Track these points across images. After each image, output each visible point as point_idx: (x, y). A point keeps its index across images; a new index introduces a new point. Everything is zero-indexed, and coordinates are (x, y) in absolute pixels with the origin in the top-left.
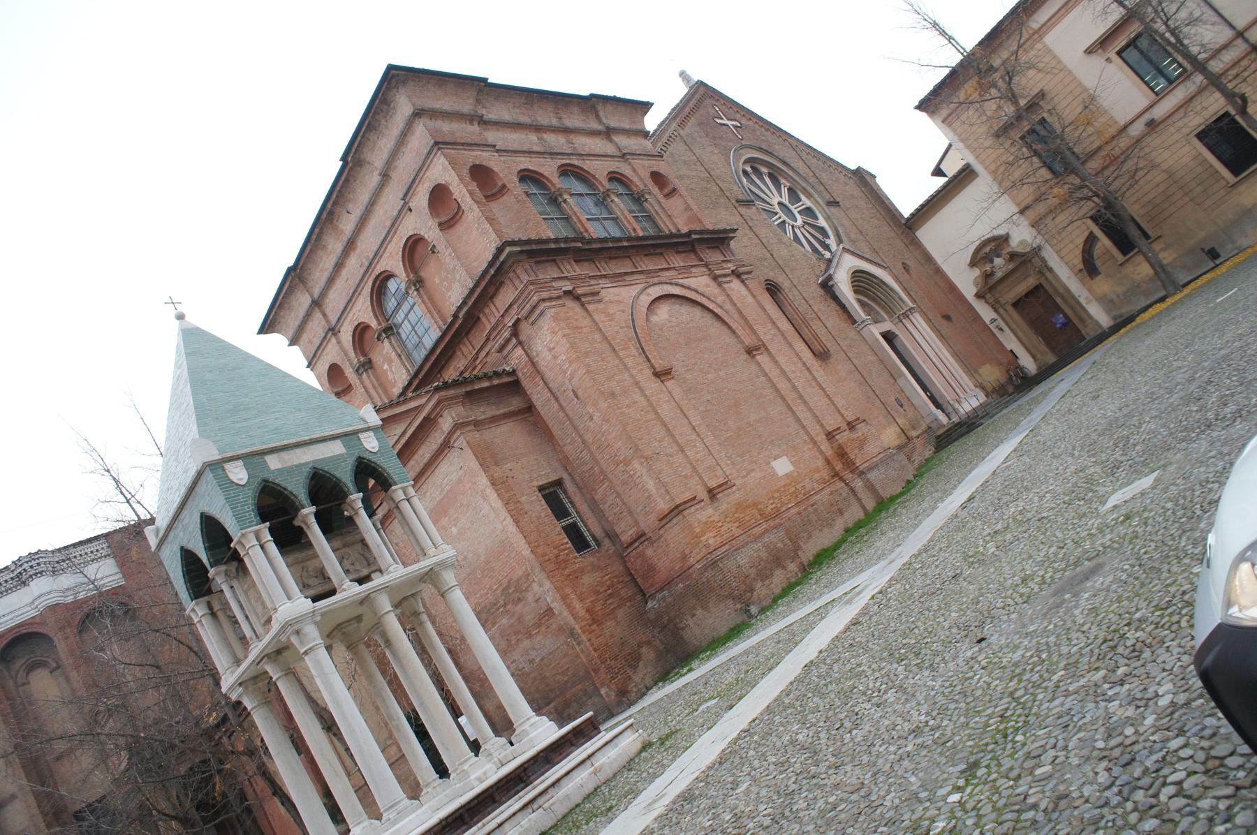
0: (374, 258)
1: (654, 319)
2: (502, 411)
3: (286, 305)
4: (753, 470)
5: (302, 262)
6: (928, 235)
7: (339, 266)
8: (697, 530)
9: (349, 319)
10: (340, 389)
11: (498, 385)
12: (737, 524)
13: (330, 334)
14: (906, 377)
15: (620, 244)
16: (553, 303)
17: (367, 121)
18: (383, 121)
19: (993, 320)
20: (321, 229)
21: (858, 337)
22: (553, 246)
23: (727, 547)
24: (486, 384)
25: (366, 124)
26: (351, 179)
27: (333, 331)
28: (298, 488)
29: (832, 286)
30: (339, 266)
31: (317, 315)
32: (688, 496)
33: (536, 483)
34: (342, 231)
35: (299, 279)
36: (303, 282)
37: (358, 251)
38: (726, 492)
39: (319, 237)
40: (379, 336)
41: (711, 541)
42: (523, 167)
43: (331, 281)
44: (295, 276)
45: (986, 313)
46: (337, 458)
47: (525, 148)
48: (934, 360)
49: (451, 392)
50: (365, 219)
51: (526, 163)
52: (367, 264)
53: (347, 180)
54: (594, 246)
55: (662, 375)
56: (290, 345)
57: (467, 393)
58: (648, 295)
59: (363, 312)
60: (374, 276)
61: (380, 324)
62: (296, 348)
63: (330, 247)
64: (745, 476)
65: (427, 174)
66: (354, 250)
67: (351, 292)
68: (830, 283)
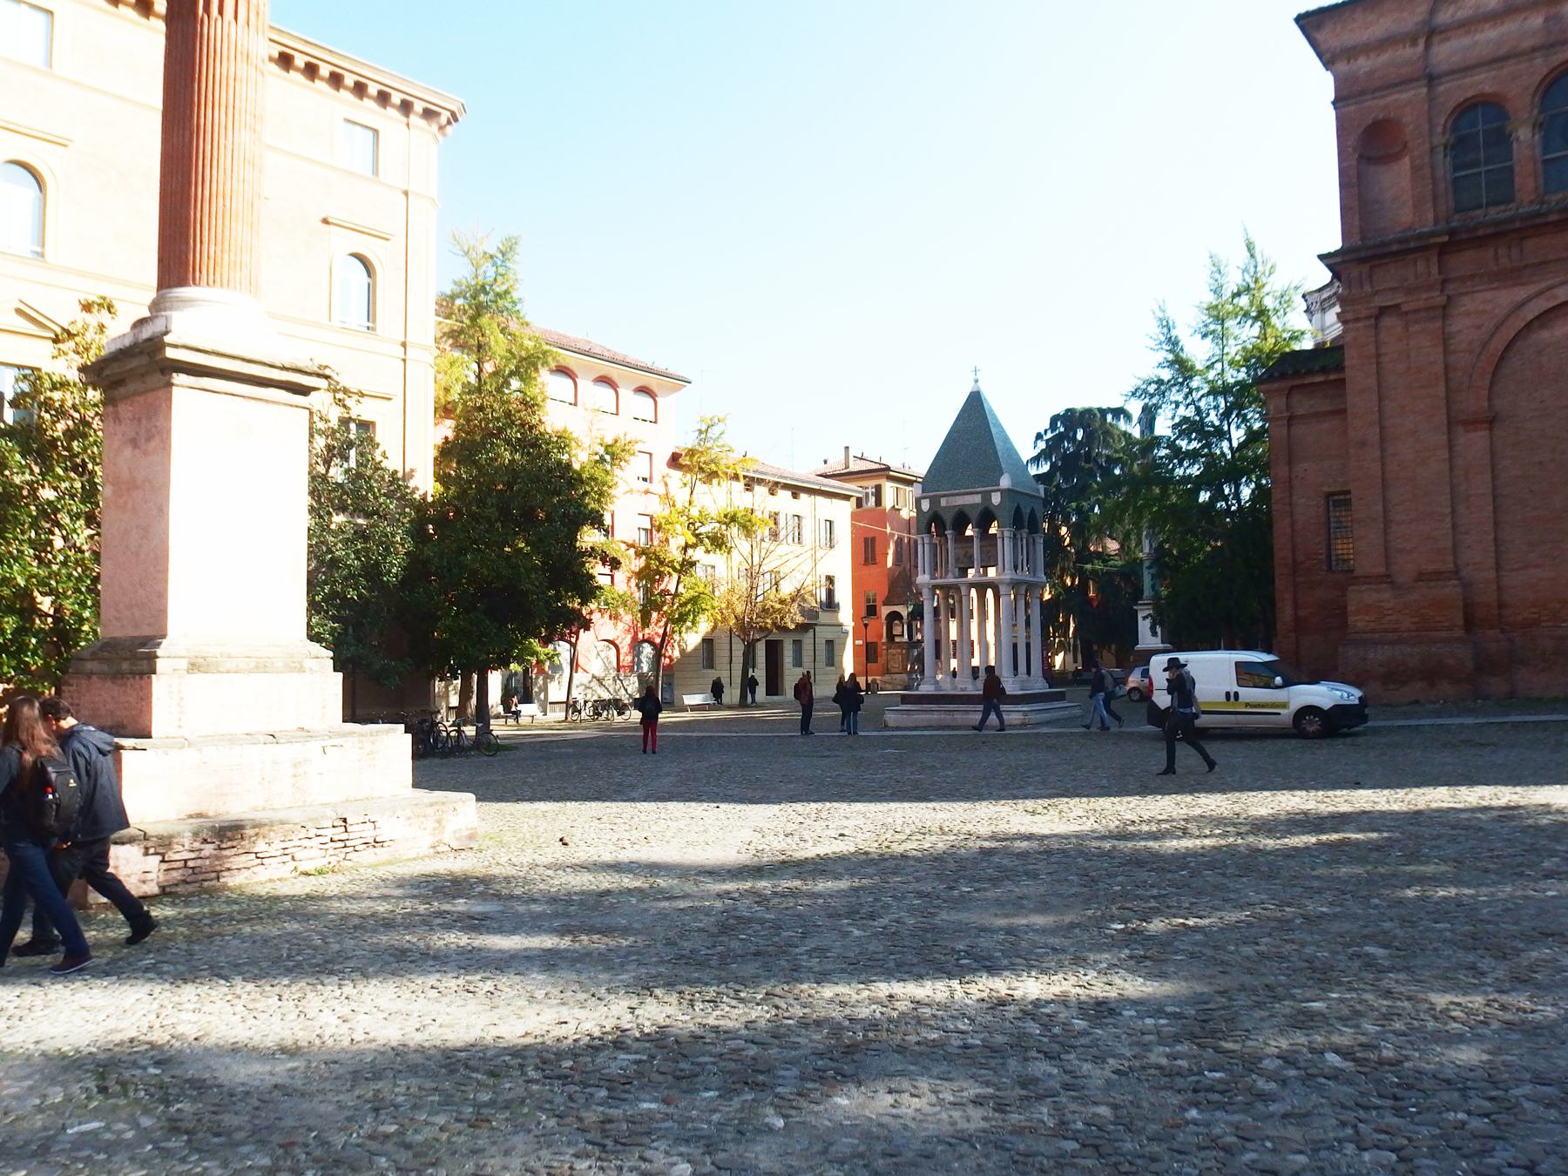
1: (1545, 335)
2: (1329, 408)
4: (1536, 566)
8: (1351, 608)
11: (1335, 380)
12: (1416, 620)
15: (1538, 221)
16: (1360, 324)
22: (1395, 248)
23: (1377, 636)
24: (1319, 379)
28: (948, 518)
32: (1382, 570)
33: (1325, 489)
38: (1432, 584)
41: (1359, 624)
42: (1470, 94)
46: (973, 506)
47: (1503, 51)
49: (1276, 385)
51: (1483, 83)
54: (1481, 232)
57: (1292, 387)
58: (1555, 297)
64: (1513, 570)
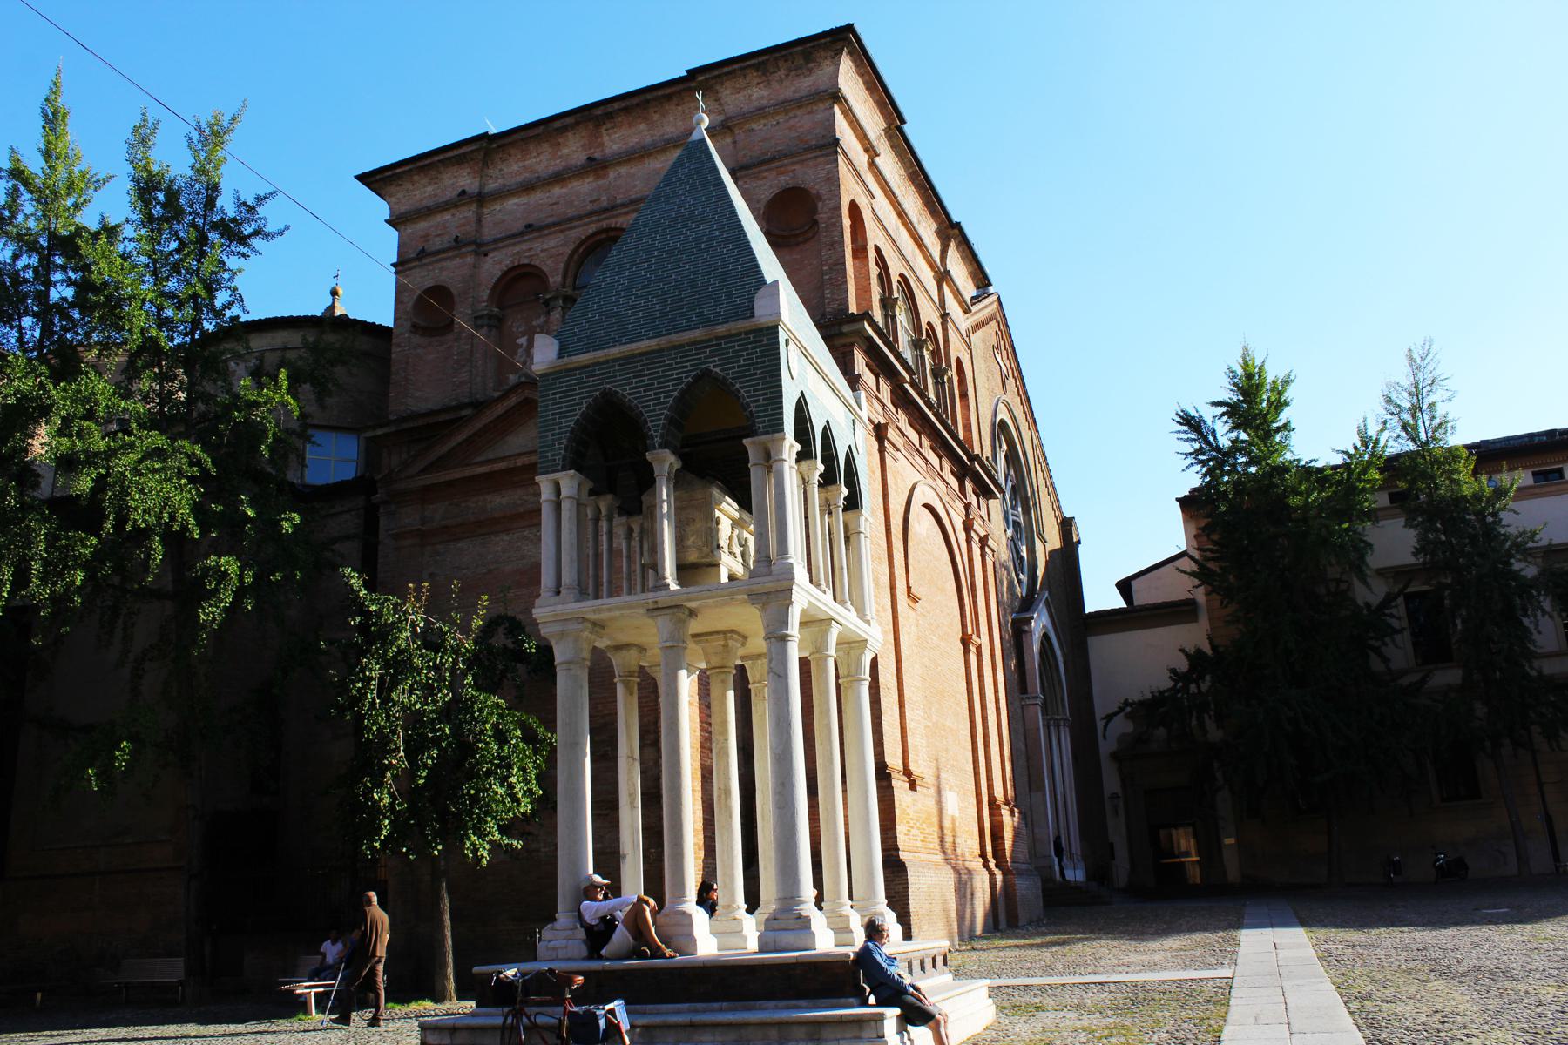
0: (623, 205)
3: (433, 173)
5: (510, 139)
6: (1102, 648)
7: (559, 178)
9: (517, 249)
10: (423, 324)
13: (473, 247)
14: (1045, 795)
17: (765, 58)
18: (782, 73)
19: (1114, 796)
20: (577, 123)
21: (1019, 711)
25: (761, 59)
26: (675, 100)
27: (481, 248)
29: (1026, 632)
30: (559, 178)
31: (468, 212)
34: (602, 144)
35: (486, 154)
36: (485, 165)
37: (601, 182)
39: (565, 129)
40: (555, 298)
43: (527, 188)
44: (484, 149)
45: (1111, 782)
48: (1059, 797)
50: (650, 155)
52: (604, 203)
53: (669, 97)
55: (913, 598)
56: (387, 221)
59: (550, 253)
60: (604, 224)
61: (564, 285)
62: (393, 235)
63: (565, 151)
65: (797, 167)
66: (598, 177)
67: (551, 220)
68: (1026, 628)
